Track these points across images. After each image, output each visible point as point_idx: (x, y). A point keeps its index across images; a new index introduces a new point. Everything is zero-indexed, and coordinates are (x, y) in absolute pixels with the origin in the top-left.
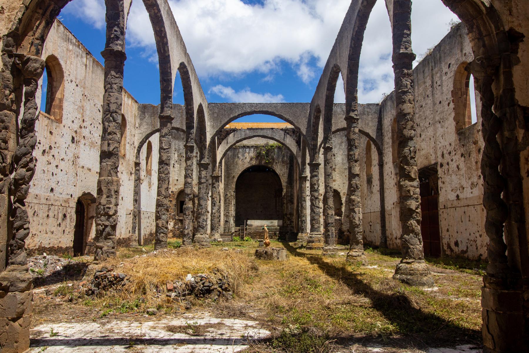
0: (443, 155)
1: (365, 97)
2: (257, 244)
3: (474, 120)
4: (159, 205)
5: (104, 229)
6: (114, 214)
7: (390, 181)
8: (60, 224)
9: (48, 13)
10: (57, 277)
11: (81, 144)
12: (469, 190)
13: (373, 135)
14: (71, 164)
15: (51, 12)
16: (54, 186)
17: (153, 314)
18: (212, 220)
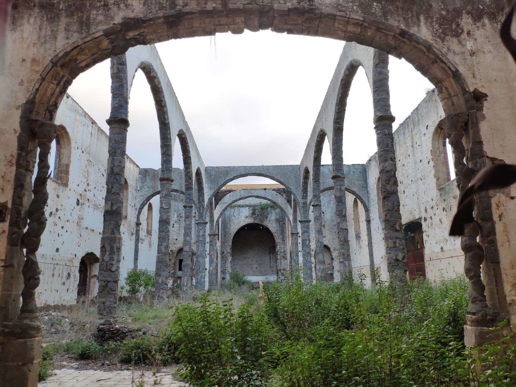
0: (426, 210)
1: (350, 158)
6: (116, 270)
8: (64, 283)
11: (85, 207)
14: (76, 224)
15: (64, 83)
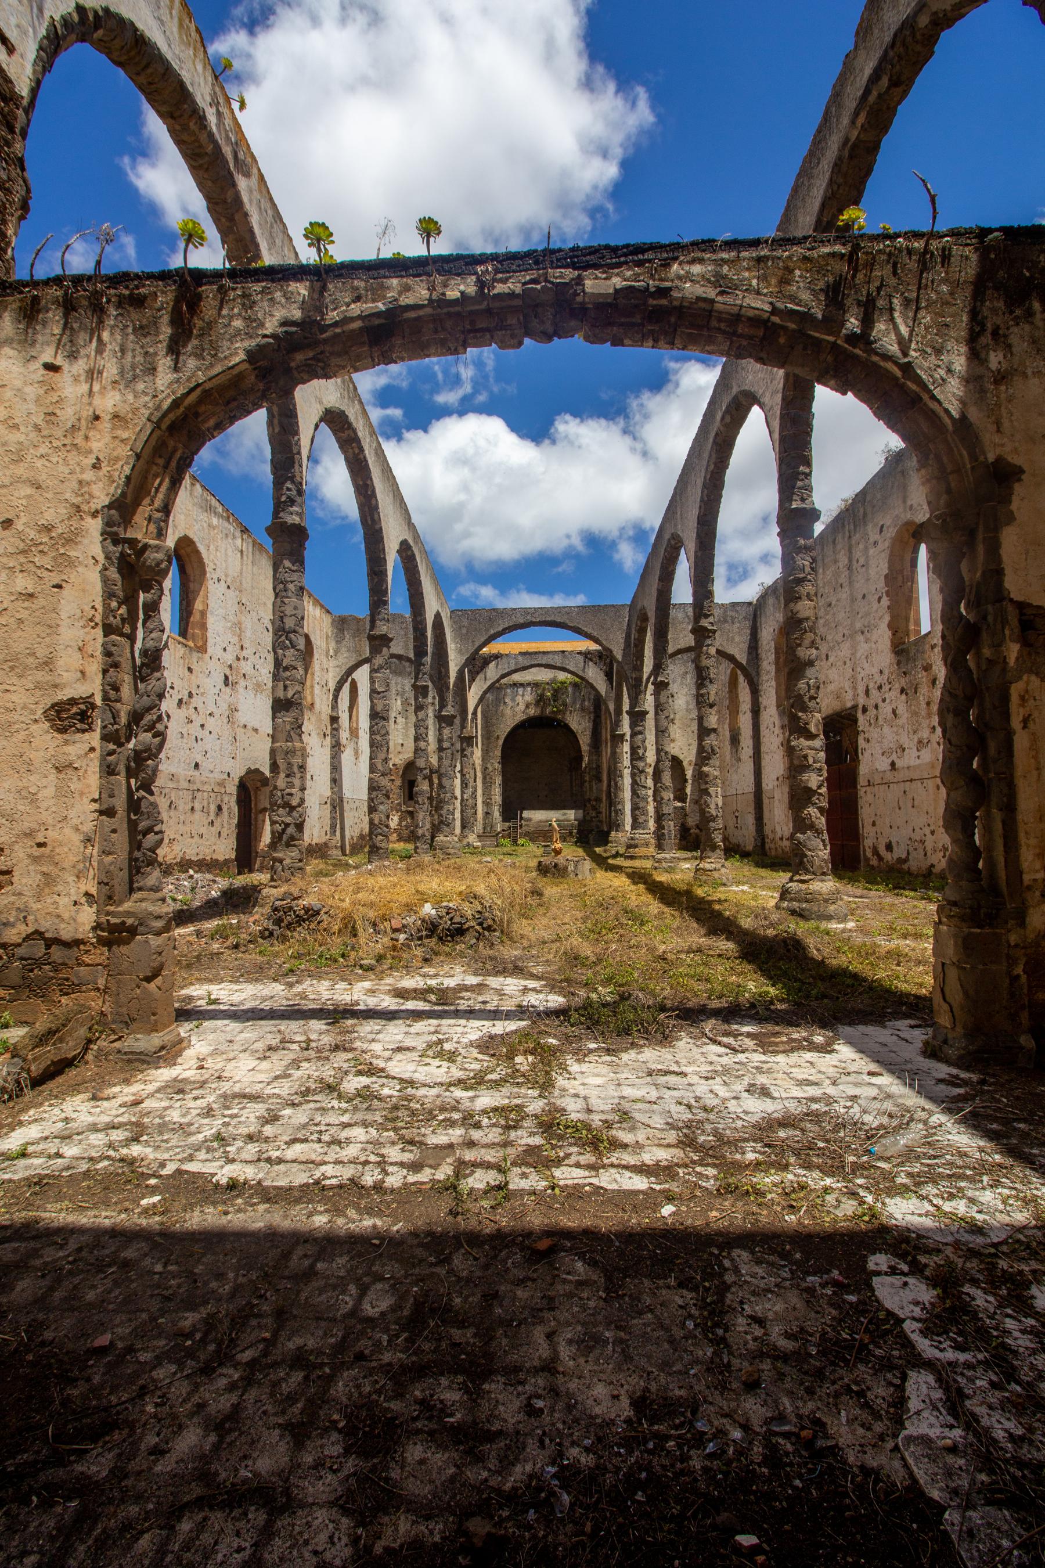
0: (867, 692)
2: (539, 852)
3: (925, 627)
4: (373, 787)
5: (284, 830)
6: (299, 805)
7: (773, 739)
9: (173, 464)
10: (212, 908)
12: (914, 753)
13: (742, 658)
14: (226, 721)
16: (199, 758)
17: (370, 968)
18: (462, 811)
